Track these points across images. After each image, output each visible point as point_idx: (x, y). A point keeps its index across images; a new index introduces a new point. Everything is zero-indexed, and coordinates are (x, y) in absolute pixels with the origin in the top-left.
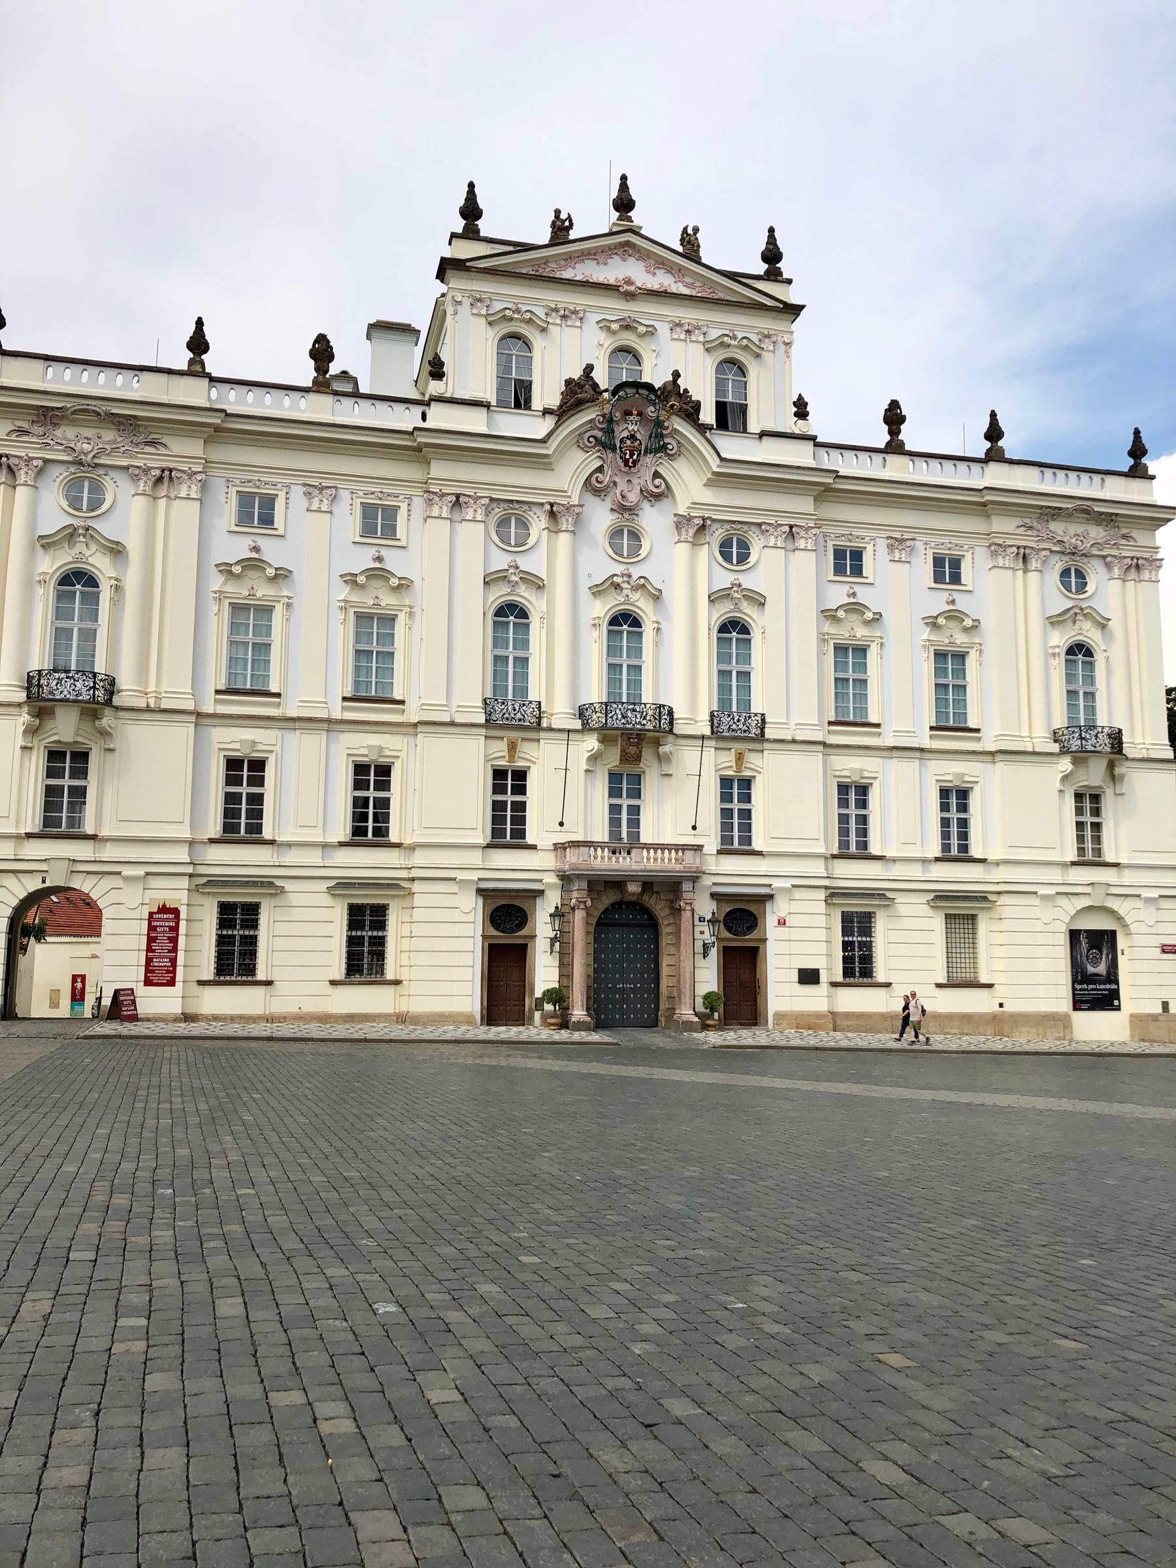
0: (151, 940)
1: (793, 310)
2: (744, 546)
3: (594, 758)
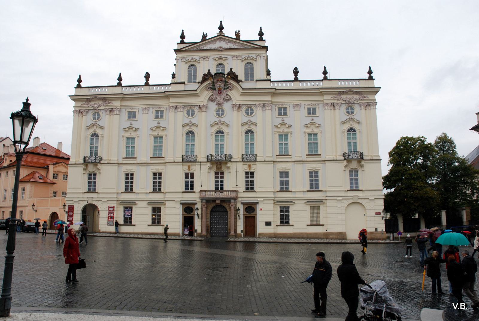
1: (266, 48)
3: (210, 168)
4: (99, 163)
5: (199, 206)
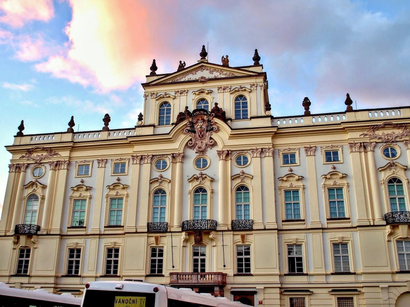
2: (245, 158)
3: (186, 241)
4: (36, 234)
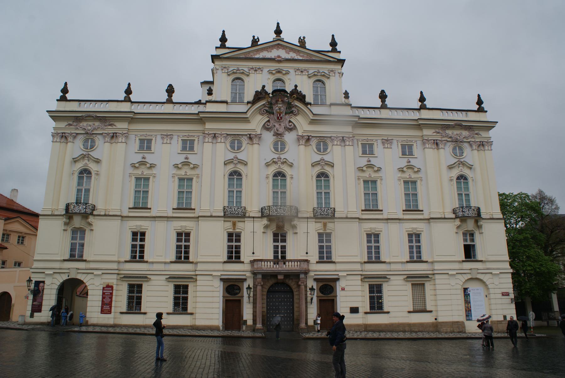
0: (103, 298)
1: (342, 62)
3: (266, 227)
4: (91, 214)
5: (250, 282)
